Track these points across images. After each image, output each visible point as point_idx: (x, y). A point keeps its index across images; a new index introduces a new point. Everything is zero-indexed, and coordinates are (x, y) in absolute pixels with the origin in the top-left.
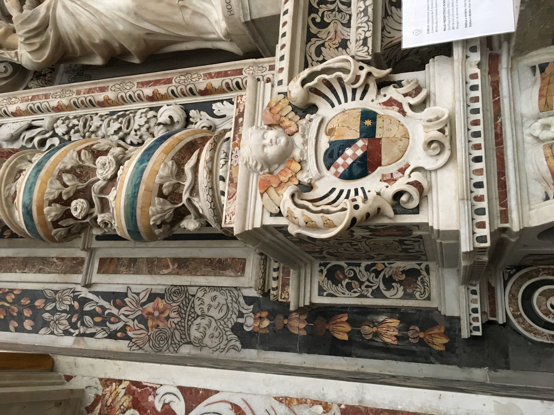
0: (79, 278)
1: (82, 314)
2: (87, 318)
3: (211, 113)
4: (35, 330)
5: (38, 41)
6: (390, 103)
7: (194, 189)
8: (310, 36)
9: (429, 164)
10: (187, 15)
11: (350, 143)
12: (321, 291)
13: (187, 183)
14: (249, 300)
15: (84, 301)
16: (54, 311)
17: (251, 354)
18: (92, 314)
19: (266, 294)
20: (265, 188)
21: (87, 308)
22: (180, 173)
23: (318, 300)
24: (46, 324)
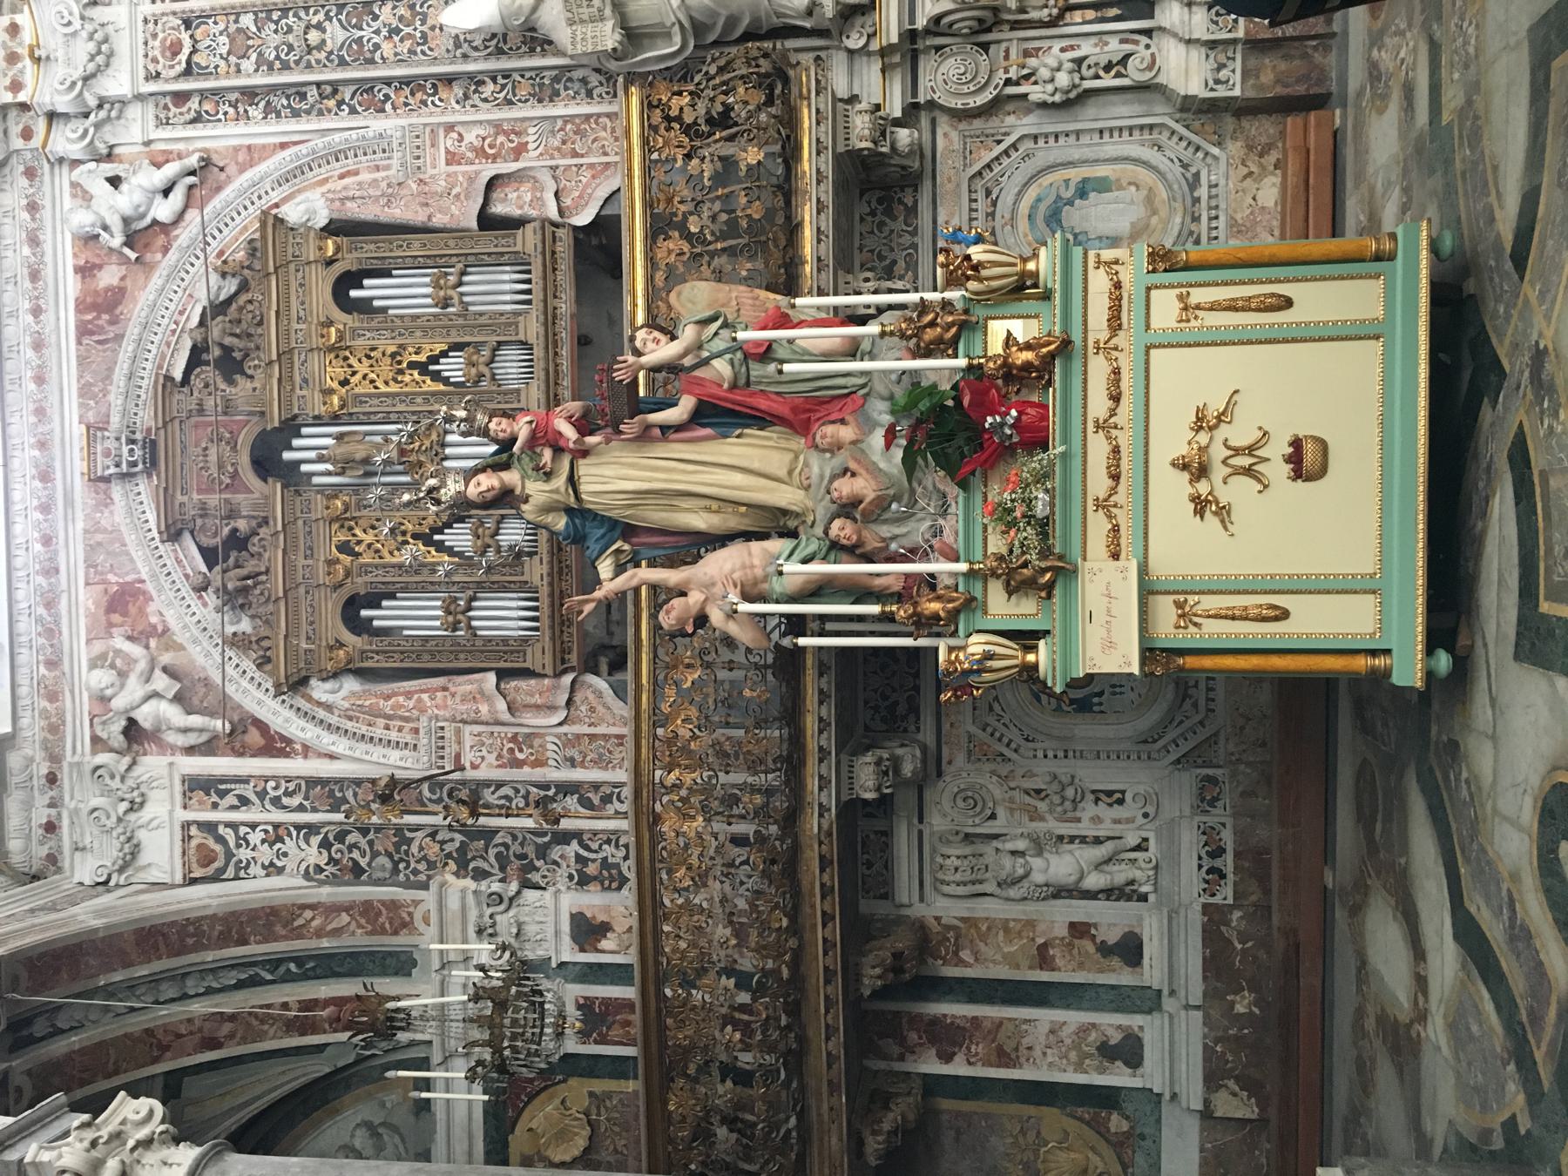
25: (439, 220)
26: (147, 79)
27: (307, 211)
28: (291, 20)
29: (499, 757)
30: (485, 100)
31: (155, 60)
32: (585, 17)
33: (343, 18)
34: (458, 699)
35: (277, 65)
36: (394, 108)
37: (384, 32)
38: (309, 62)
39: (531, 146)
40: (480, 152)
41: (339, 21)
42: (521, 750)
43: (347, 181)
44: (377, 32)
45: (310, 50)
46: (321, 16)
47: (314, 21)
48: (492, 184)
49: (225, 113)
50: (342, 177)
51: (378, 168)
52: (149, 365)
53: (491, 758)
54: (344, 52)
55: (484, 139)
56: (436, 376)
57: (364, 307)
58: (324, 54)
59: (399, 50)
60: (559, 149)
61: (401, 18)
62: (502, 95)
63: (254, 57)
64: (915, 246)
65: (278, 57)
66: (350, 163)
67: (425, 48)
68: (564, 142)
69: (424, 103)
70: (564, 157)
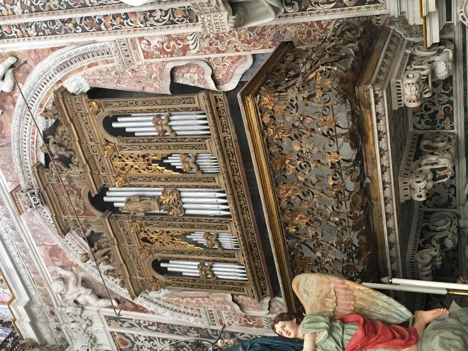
25: (148, 90)
27: (77, 86)
29: (240, 322)
30: (157, 21)
32: (208, 11)
34: (215, 302)
35: (33, 9)
36: (106, 27)
38: (50, 6)
39: (191, 47)
40: (162, 51)
42: (250, 321)
43: (93, 69)
48: (173, 71)
49: (16, 32)
50: (89, 66)
51: (107, 62)
52: (28, 158)
53: (237, 322)
55: (163, 43)
56: (169, 166)
57: (121, 132)
60: (208, 49)
62: (167, 18)
64: (451, 103)
65: (32, 4)
66: (91, 60)
68: (211, 44)
69: (122, 24)
70: (212, 52)
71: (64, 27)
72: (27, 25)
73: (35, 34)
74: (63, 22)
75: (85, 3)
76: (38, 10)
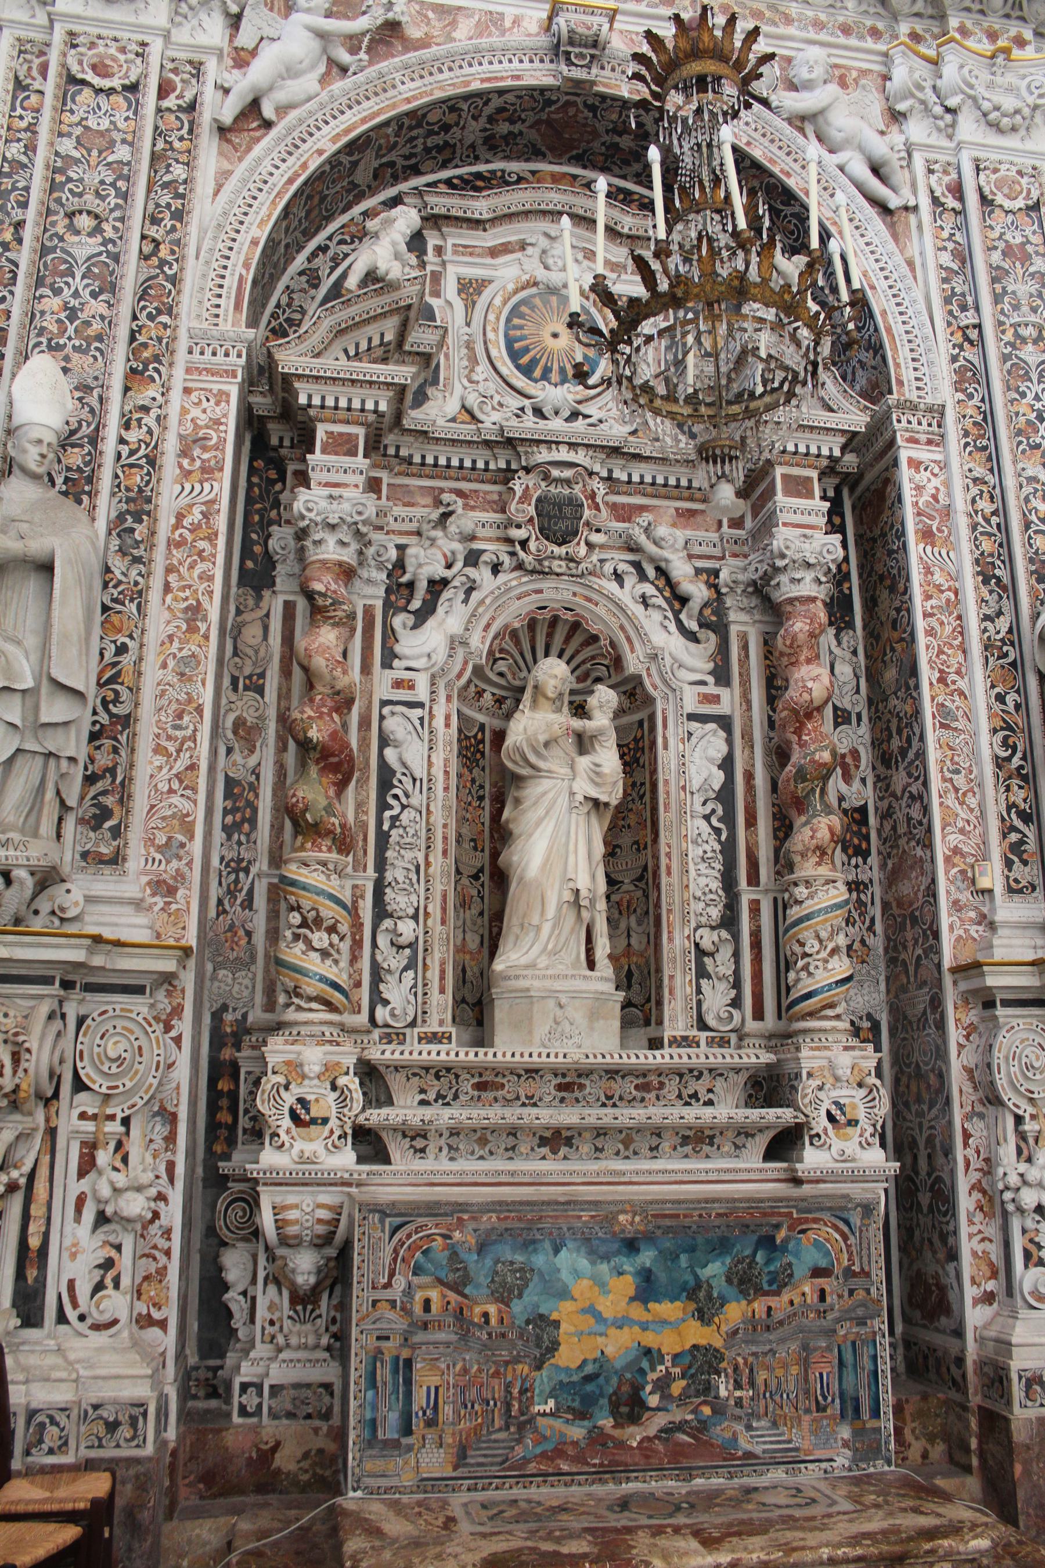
0: (265, 867)
1: (236, 871)
2: (233, 877)
3: (405, 969)
4: (225, 828)
5: (518, 758)
6: (332, 1132)
7: (299, 1008)
8: (427, 1069)
9: (295, 1152)
10: (516, 930)
11: (308, 1111)
12: (249, 1073)
13: (303, 1004)
14: (245, 1016)
15: (247, 871)
16: (239, 843)
17: (207, 1020)
18: (237, 881)
19: (248, 1032)
20: (288, 1063)
21: (242, 875)
22: (310, 999)
23: (243, 1071)
24: (229, 837)
26: (71, 34)
28: (113, 201)
31: (92, 45)
33: (103, 258)
35: (59, 178)
37: (74, 303)
38: (57, 213)
41: (100, 254)
44: (76, 294)
45: (70, 216)
46: (110, 233)
47: (105, 226)
49: (21, 118)
54: (59, 253)
58: (61, 231)
59: (48, 317)
61: (87, 324)
63: (77, 154)
65: (69, 180)
67: (44, 347)
71: (7, 221)
72: (31, 148)
73: (8, 155)
74: (19, 225)
75: (43, 285)
76: (54, 187)
